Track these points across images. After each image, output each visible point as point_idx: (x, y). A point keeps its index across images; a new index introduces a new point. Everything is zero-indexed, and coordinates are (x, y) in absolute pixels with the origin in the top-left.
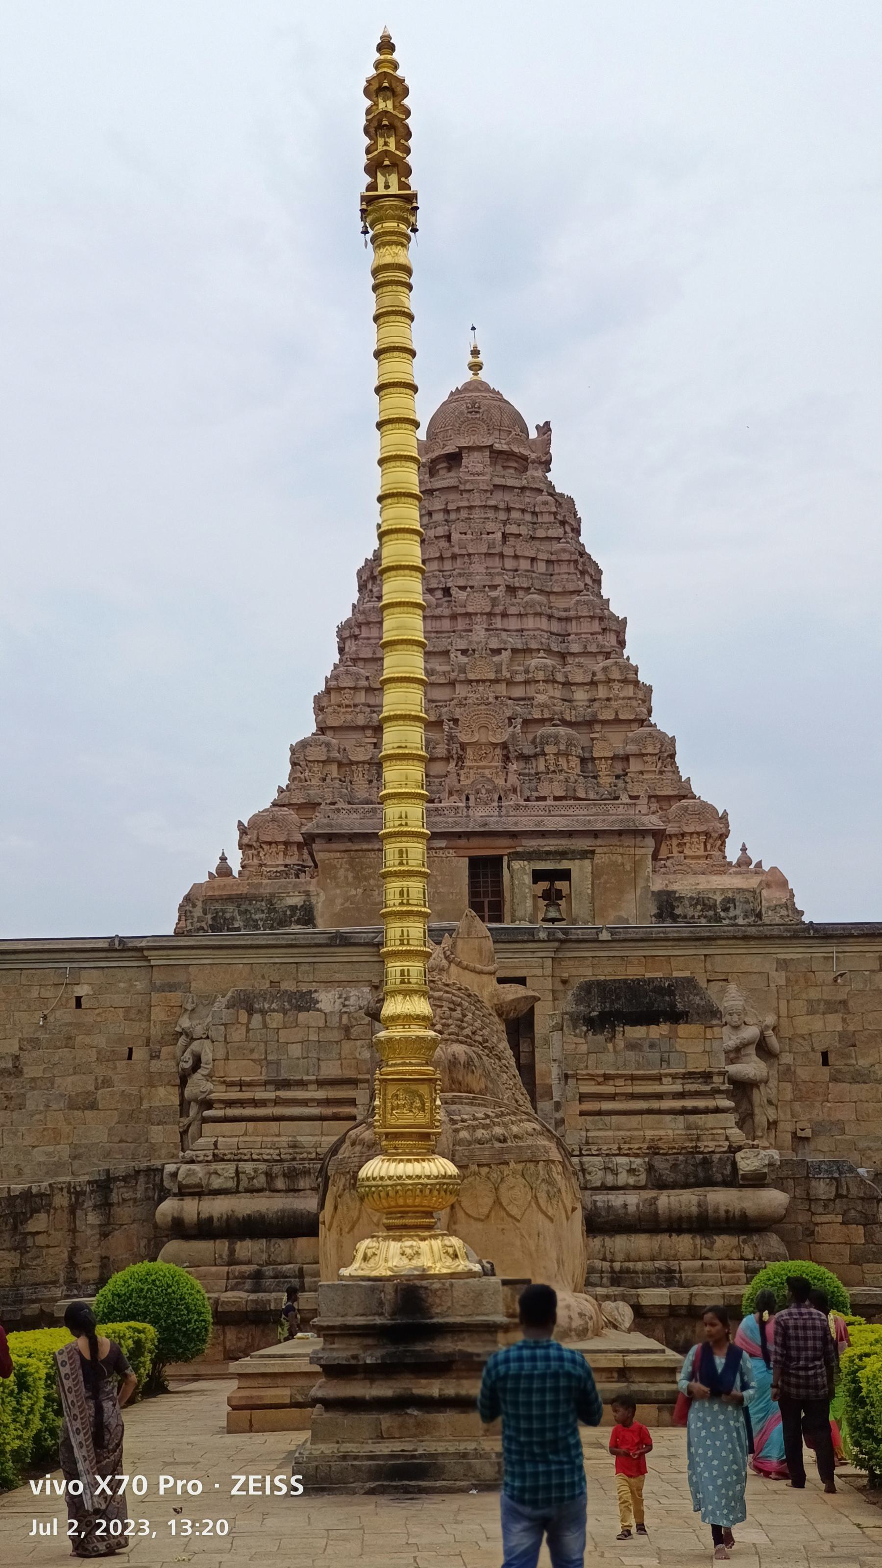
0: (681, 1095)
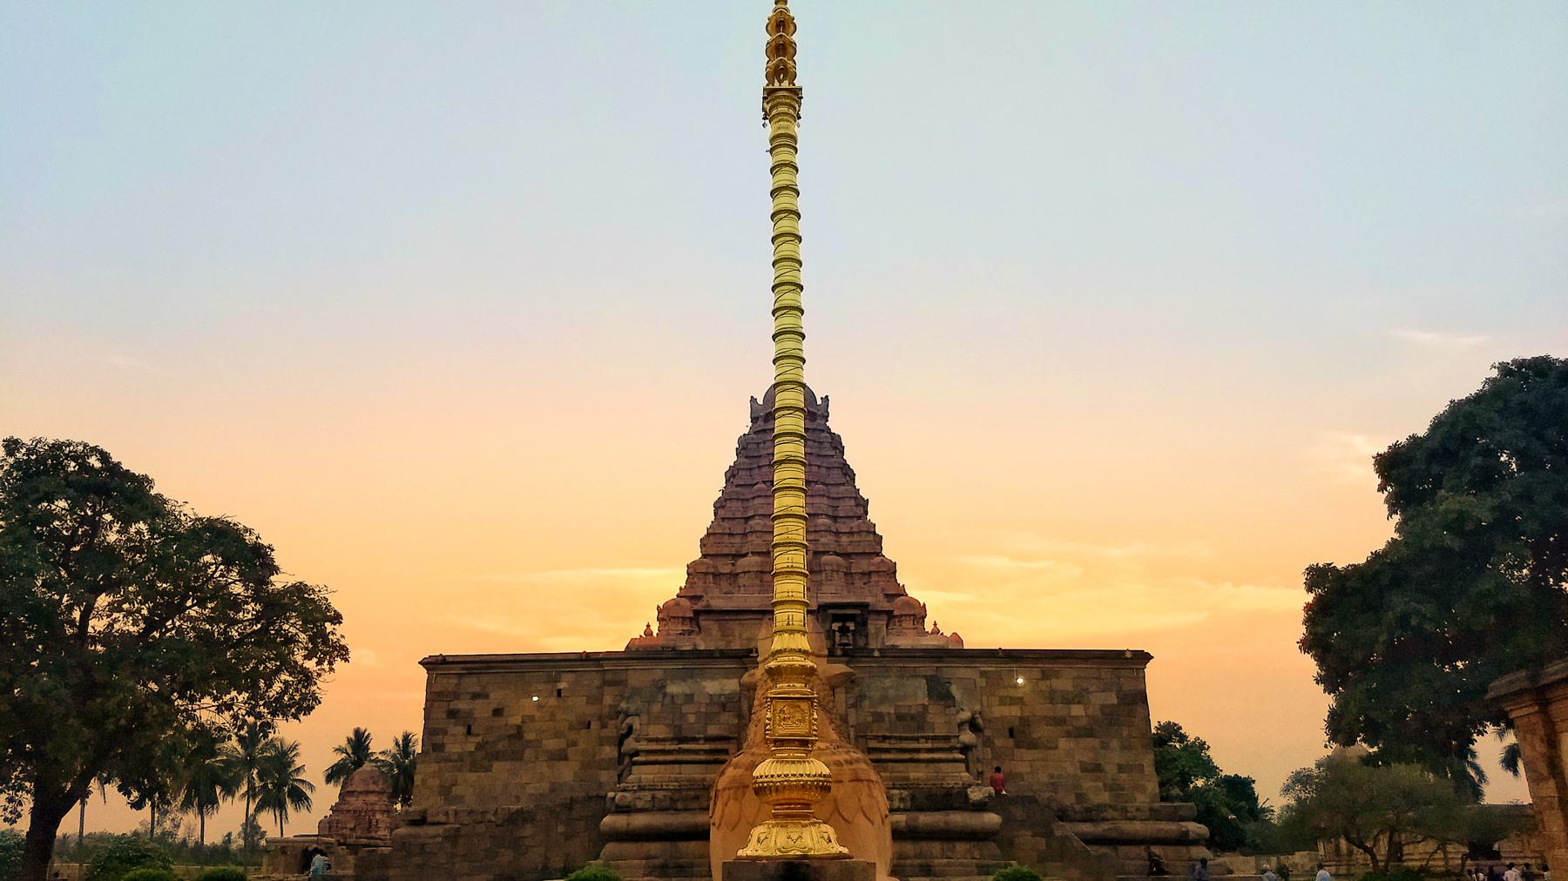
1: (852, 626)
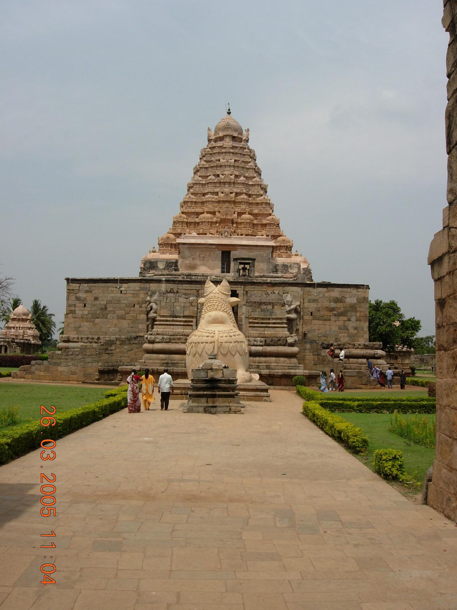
0: (275, 323)
1: (247, 266)
